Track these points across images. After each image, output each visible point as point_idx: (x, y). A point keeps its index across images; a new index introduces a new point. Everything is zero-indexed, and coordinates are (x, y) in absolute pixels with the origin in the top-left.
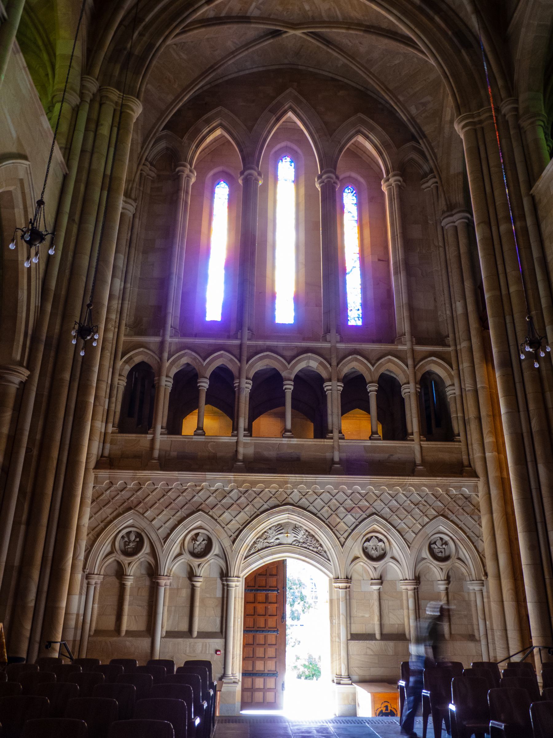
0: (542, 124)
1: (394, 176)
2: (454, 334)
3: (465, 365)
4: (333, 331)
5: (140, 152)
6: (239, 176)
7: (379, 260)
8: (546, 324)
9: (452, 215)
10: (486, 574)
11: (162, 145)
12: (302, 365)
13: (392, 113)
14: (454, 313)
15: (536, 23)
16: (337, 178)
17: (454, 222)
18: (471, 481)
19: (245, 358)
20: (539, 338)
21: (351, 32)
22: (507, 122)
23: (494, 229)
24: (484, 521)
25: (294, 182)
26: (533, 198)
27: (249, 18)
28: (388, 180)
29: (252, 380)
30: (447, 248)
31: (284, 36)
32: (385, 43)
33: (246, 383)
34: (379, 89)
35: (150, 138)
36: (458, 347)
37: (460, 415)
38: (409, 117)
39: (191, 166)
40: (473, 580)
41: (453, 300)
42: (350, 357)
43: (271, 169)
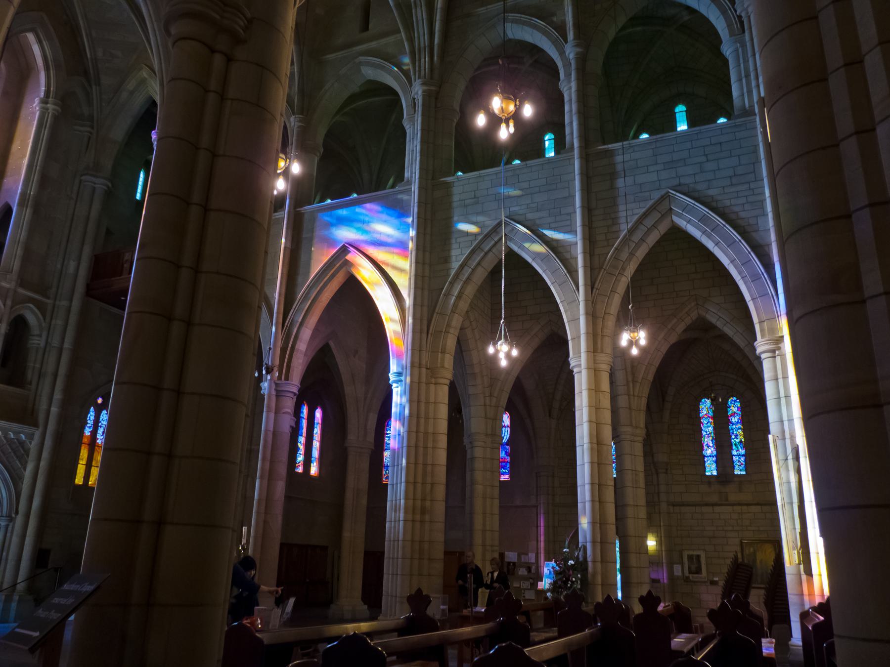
1: (55, 104)
2: (58, 288)
3: (59, 322)
10: (17, 513)
17: (95, 183)
18: (28, 429)
24: (30, 467)
36: (57, 303)
37: (38, 366)
40: (3, 517)
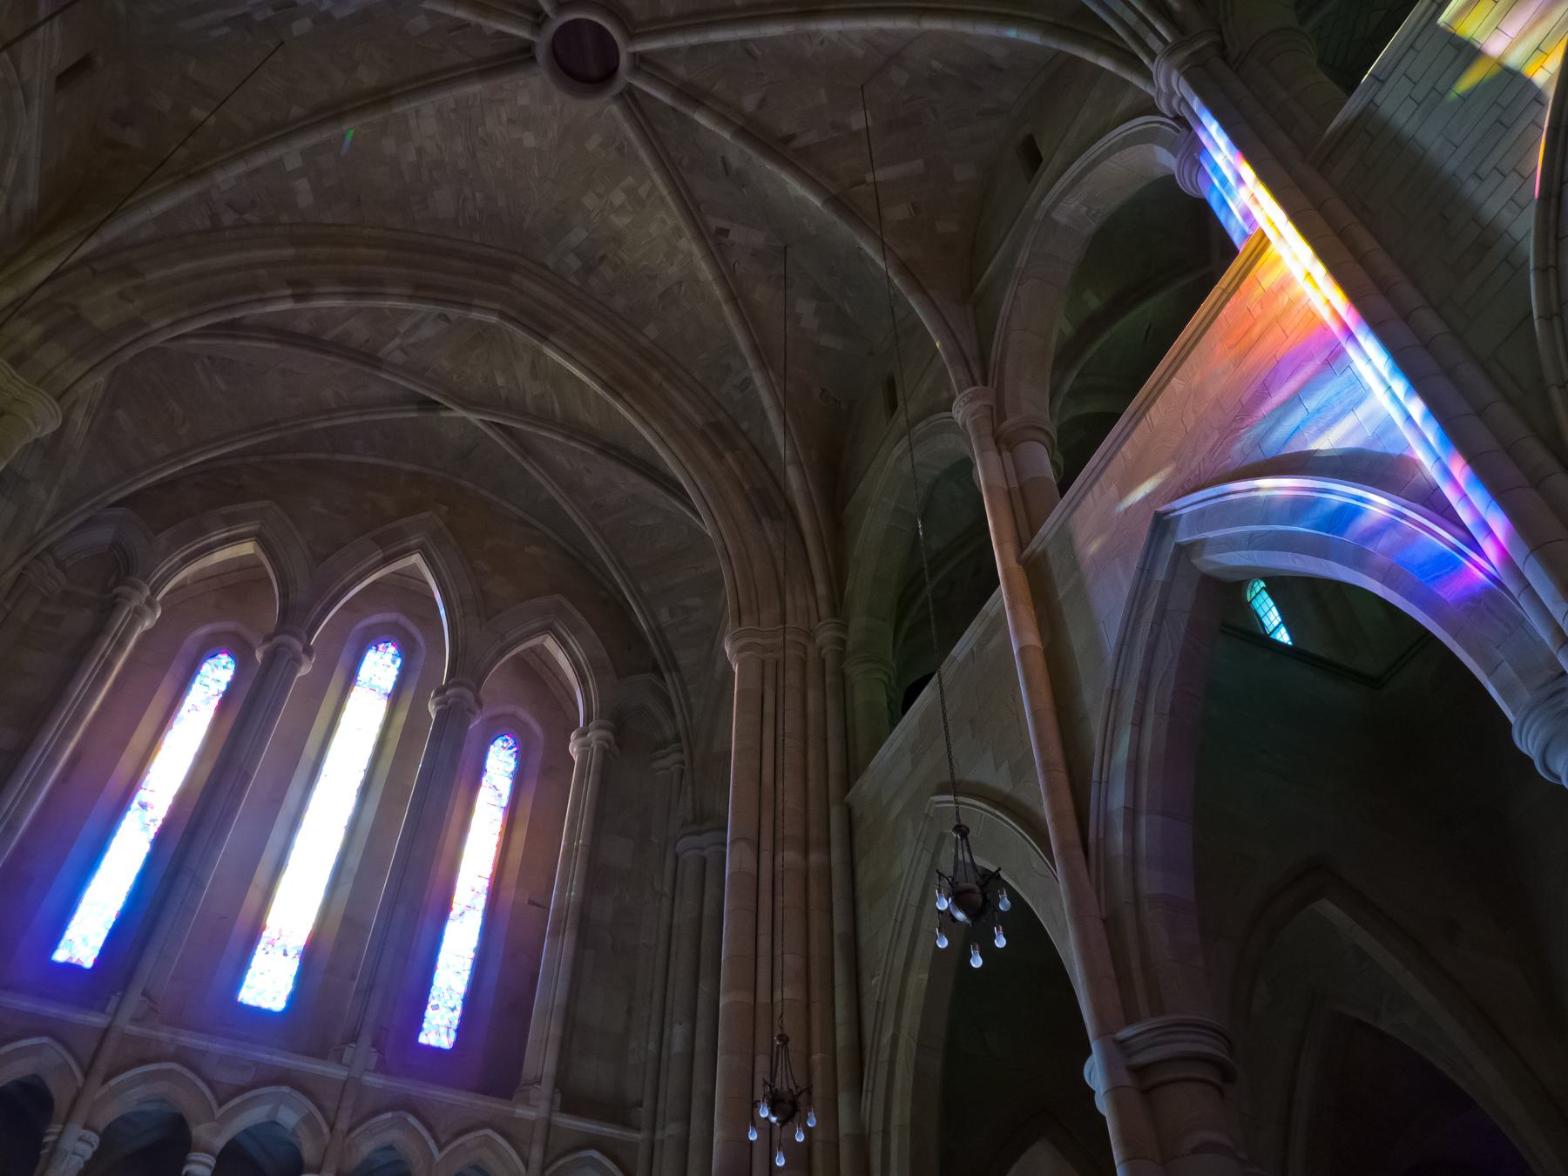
0: (886, 679)
1: (599, 727)
4: (365, 1040)
5: (40, 531)
6: (261, 642)
7: (531, 903)
8: (840, 1085)
9: (699, 833)
11: (103, 535)
12: (255, 1115)
13: (624, 611)
14: (665, 1051)
15: (894, 503)
16: (479, 703)
17: (702, 849)
19: (102, 1066)
20: (795, 1093)
21: (573, 444)
22: (824, 660)
23: (766, 856)
25: (389, 695)
26: (849, 812)
27: (380, 360)
28: (583, 734)
29: (100, 1136)
30: (677, 900)
31: (444, 414)
32: (632, 482)
33: (80, 1139)
34: (606, 560)
35: (76, 511)
36: (658, 1136)
38: (653, 626)
39: (154, 591)
41: (667, 1018)
42: (389, 1115)
43: (346, 658)
